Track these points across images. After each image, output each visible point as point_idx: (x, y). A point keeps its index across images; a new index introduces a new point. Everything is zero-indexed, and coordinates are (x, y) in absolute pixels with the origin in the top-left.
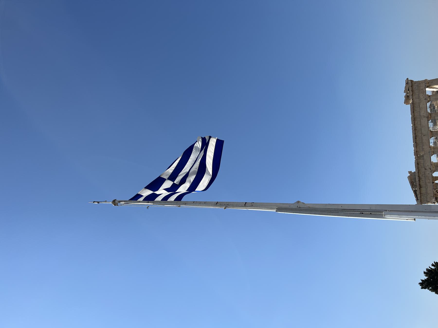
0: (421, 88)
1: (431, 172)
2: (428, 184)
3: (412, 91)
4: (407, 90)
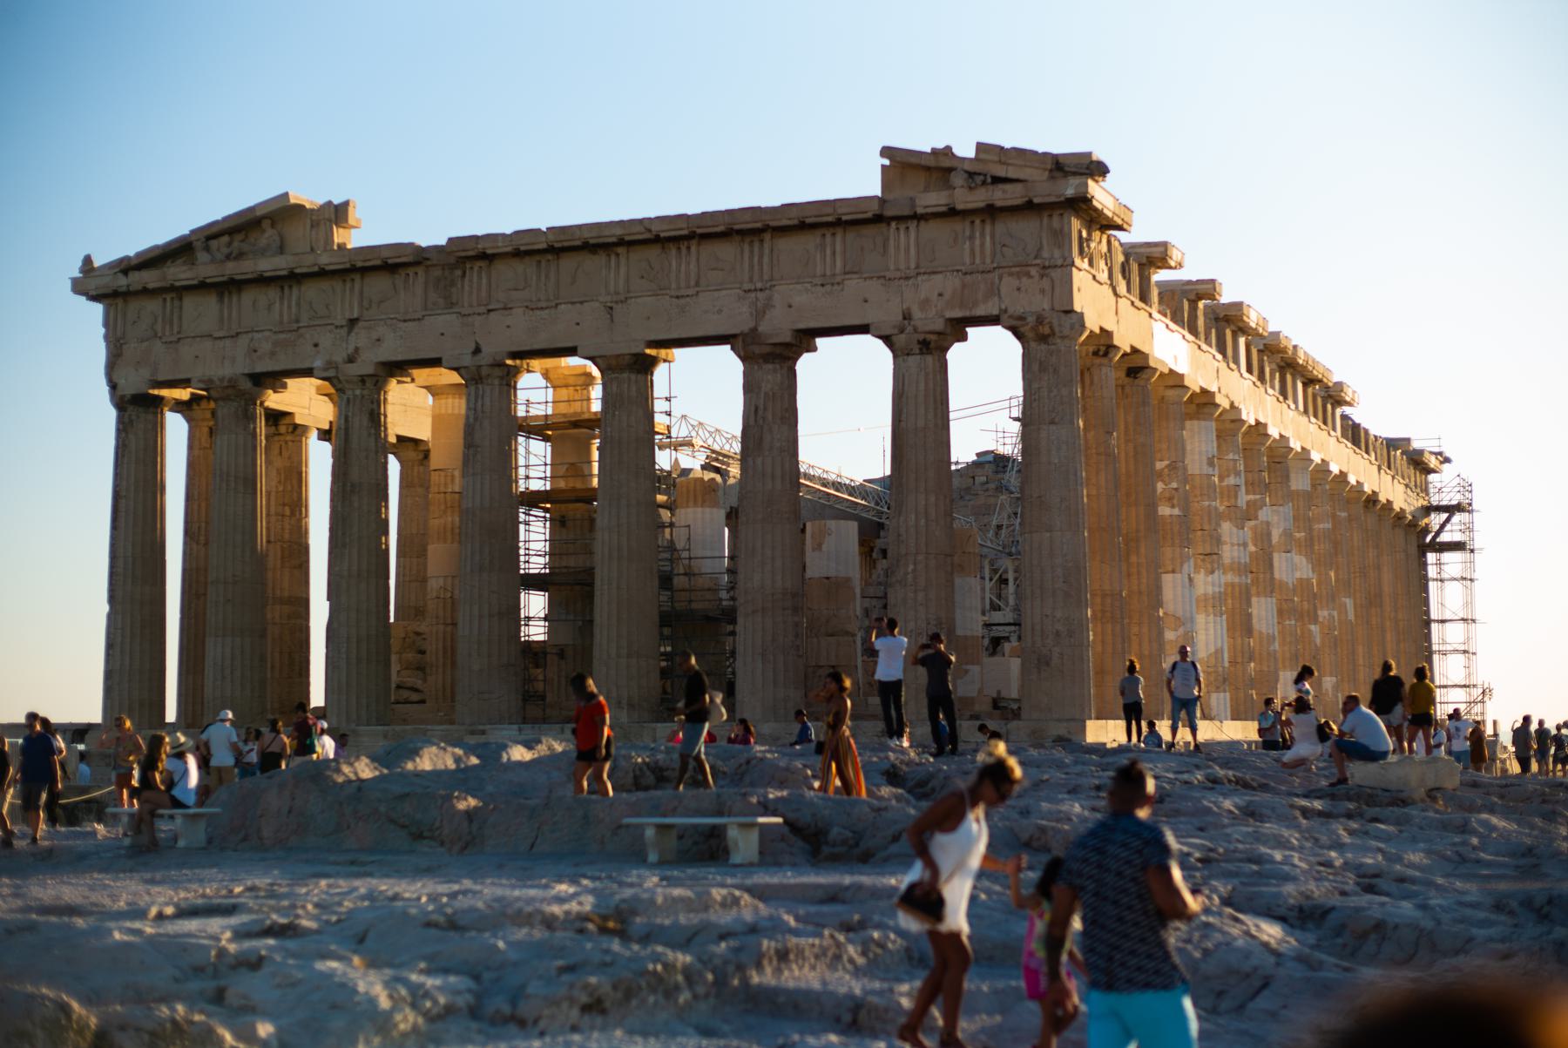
0: (1008, 284)
1: (330, 365)
2: (244, 341)
3: (991, 212)
4: (996, 165)
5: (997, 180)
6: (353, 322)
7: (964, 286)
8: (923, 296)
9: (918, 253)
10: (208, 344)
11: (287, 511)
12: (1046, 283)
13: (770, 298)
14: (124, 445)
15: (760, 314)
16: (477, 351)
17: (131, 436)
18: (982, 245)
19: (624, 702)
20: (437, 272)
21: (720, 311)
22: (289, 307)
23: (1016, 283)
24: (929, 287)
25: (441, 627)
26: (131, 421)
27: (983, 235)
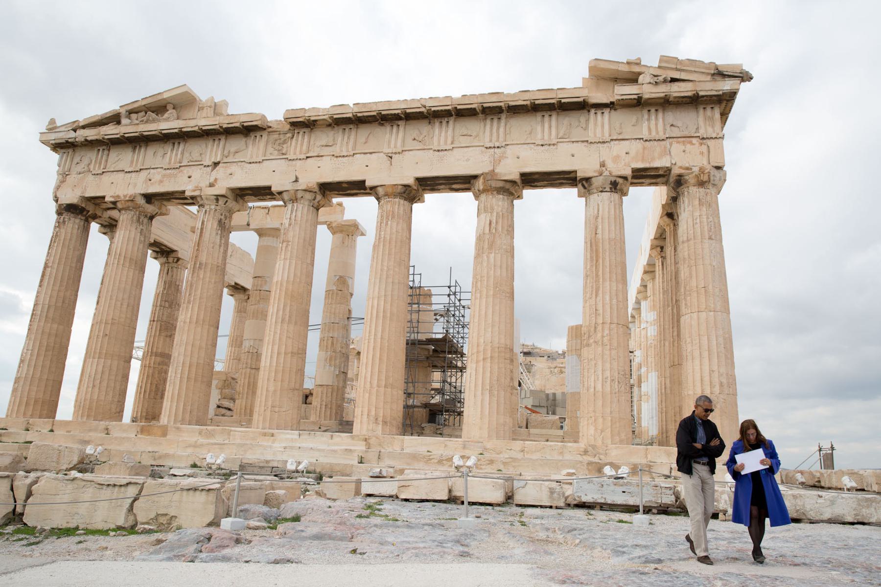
0: (676, 148)
2: (144, 174)
5: (673, 80)
6: (216, 164)
7: (644, 148)
8: (615, 154)
9: (610, 128)
10: (121, 175)
11: (167, 305)
12: (704, 148)
13: (505, 153)
14: (57, 235)
15: (497, 162)
16: (296, 181)
17: (63, 231)
18: (656, 125)
19: (380, 419)
20: (276, 136)
21: (468, 160)
22: (176, 155)
23: (683, 148)
24: (619, 148)
25: (248, 370)
26: (64, 222)
27: (656, 118)
